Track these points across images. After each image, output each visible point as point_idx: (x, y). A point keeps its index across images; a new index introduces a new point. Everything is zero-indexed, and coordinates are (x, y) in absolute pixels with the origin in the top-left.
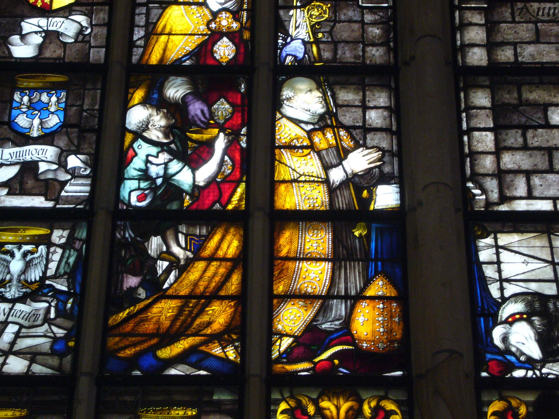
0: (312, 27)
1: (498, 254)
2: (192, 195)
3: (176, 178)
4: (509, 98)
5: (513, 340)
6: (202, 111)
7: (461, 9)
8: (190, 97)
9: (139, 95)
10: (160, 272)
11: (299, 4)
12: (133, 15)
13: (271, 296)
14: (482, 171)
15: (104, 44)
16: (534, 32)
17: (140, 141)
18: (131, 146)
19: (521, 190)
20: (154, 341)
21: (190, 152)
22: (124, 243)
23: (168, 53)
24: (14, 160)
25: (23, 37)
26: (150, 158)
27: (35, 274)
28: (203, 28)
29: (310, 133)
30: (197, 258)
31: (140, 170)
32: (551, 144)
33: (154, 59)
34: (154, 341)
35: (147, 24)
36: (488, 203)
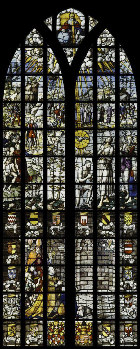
1: (79, 299)
4: (82, 270)
5: (80, 313)
8: (34, 271)
10: (32, 302)
14: (77, 285)
17: (27, 279)
18: (26, 280)
19: (83, 288)
20: (32, 314)
22: (27, 298)
24: (9, 283)
25: (8, 259)
27: (14, 303)
29: (52, 277)
30: (36, 300)
32: (88, 280)
34: (32, 314)
35: (27, 257)
36: (78, 291)
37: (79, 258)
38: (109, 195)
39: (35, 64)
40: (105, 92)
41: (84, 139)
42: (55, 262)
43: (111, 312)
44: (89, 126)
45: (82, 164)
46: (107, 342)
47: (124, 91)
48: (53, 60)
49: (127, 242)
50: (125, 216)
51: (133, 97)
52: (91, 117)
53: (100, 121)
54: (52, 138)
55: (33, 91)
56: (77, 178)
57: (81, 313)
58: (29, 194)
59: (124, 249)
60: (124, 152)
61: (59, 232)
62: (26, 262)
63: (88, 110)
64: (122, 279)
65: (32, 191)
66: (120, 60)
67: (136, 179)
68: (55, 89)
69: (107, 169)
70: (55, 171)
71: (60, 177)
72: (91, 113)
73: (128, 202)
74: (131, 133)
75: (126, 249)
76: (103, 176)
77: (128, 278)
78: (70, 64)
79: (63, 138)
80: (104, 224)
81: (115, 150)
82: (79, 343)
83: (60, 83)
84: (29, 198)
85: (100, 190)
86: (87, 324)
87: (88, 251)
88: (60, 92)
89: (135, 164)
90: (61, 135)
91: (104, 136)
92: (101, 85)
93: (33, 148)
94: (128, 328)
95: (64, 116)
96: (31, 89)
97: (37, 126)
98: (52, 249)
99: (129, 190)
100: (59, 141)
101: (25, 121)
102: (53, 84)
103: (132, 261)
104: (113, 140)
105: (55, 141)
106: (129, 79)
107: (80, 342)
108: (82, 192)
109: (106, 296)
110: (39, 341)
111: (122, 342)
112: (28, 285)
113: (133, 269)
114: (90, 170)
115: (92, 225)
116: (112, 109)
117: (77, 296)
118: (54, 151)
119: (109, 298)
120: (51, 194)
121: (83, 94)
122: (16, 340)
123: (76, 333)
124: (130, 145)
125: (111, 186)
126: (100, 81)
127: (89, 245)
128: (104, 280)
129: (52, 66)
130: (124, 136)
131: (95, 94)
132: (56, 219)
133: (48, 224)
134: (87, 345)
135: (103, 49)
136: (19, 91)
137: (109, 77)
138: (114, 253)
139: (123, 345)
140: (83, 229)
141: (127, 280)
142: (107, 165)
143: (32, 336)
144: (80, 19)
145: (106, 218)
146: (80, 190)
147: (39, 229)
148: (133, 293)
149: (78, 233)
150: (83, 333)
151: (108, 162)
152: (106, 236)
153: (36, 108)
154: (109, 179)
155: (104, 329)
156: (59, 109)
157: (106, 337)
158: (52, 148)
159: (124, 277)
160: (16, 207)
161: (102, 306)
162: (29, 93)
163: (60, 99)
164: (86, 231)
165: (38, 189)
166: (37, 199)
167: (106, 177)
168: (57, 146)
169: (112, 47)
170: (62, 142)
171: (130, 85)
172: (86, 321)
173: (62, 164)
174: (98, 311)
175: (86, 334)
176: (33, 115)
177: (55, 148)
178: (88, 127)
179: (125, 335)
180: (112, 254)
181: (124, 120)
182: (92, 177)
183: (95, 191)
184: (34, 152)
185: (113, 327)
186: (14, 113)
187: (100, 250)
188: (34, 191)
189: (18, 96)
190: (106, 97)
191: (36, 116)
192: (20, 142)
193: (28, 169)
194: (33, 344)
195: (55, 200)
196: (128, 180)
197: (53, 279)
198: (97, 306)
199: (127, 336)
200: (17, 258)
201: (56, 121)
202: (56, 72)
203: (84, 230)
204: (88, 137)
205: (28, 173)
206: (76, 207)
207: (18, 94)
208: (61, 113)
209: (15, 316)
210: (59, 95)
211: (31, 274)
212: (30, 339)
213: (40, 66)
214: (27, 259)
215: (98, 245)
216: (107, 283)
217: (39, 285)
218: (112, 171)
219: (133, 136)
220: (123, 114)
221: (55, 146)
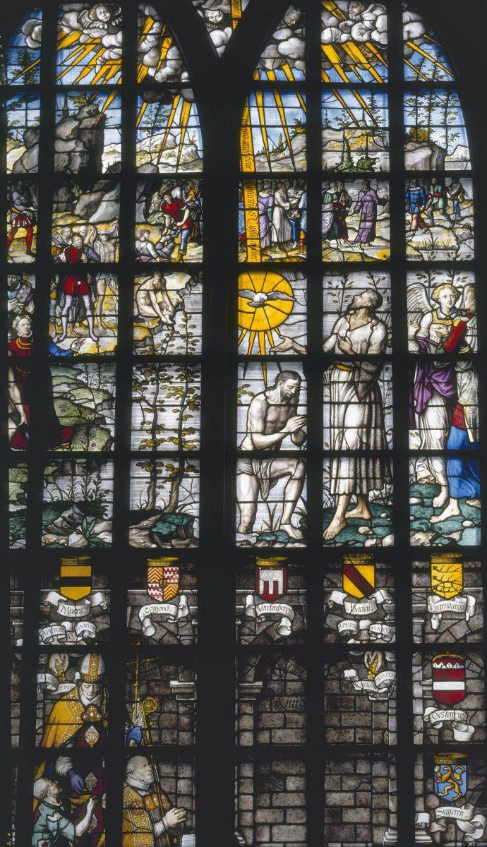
0: (146, 717)
2: (74, 843)
3: (64, 831)
4: (264, 770)
6: (79, 782)
7: (240, 702)
9: (42, 769)
11: (138, 700)
14: (244, 824)
15: (18, 732)
16: (283, 720)
21: (72, 812)
23: (57, 739)
26: (49, 817)
28: (78, 718)
31: (43, 826)
33: (49, 745)
37: (251, 722)
38: (371, 494)
39: (93, 54)
40: (351, 141)
41: (274, 300)
44: (289, 254)
45: (266, 385)
48: (157, 39)
49: (445, 661)
50: (435, 568)
51: (454, 157)
52: (300, 225)
53: (330, 235)
54: (152, 294)
55: (85, 139)
56: (247, 433)
58: (60, 490)
59: (432, 685)
60: (424, 342)
61: (172, 628)
63: (288, 201)
64: (425, 802)
65: (72, 480)
66: (405, 37)
67: (474, 437)
68: (165, 133)
70: (163, 410)
71: (180, 431)
72: (300, 211)
73: (442, 517)
74: (453, 277)
75: (440, 686)
76: (348, 424)
77: (453, 795)
78: (220, 50)
79: (192, 296)
80: (349, 595)
81: (393, 333)
83: (184, 113)
84: (60, 506)
85: (334, 476)
87: (286, 695)
89: (467, 386)
90: (188, 284)
91: (347, 286)
92: (337, 119)
93: (79, 330)
95: (198, 220)
96: (78, 134)
97: (95, 256)
98: (143, 688)
99: (446, 477)
100: (179, 307)
101: (50, 239)
102: (157, 115)
103: (466, 731)
104: (385, 302)
105: (164, 305)
106: (438, 100)
108: (265, 485)
112: (46, 826)
114: (296, 405)
115: (301, 601)
116: (377, 197)
118: (158, 339)
120: (145, 492)
121: (271, 150)
124: (448, 318)
125: (378, 464)
126: (331, 105)
127: (291, 673)
128: (352, 803)
129: (154, 58)
130: (425, 287)
131: (315, 148)
132: (164, 578)
133: (131, 597)
136: (33, 138)
138: (393, 704)
140: (269, 616)
141: (444, 802)
142: (360, 386)
145: (360, 574)
146: (256, 476)
147: (92, 616)
149: (247, 631)
151: (364, 376)
152: (356, 637)
153: (93, 197)
154: (368, 437)
158: (150, 330)
159: (433, 793)
163: (186, 164)
164: (280, 621)
165: (96, 473)
166: (91, 508)
167: (358, 428)
168: (170, 322)
170: (188, 307)
171: (445, 120)
173: (191, 385)
176: (81, 218)
177: (165, 327)
178: (288, 257)
180: (383, 708)
181: (425, 233)
182: (305, 429)
183: (313, 481)
184: (81, 343)
186: (12, 212)
187: (337, 691)
188: (79, 479)
189: (27, 154)
190: (356, 158)
191: (92, 220)
192: (31, 309)
193: (58, 406)
195: (160, 512)
196: (445, 440)
201: (168, 237)
202: (169, 77)
203: (274, 619)
204: (288, 290)
205: (56, 418)
206: (240, 537)
207: (29, 148)
208: (187, 213)
210: (180, 151)
213: (111, 59)
214: (44, 727)
215: (326, 674)
216: (364, 815)
218: (383, 409)
219: (461, 287)
220: (420, 213)
221: (161, 323)
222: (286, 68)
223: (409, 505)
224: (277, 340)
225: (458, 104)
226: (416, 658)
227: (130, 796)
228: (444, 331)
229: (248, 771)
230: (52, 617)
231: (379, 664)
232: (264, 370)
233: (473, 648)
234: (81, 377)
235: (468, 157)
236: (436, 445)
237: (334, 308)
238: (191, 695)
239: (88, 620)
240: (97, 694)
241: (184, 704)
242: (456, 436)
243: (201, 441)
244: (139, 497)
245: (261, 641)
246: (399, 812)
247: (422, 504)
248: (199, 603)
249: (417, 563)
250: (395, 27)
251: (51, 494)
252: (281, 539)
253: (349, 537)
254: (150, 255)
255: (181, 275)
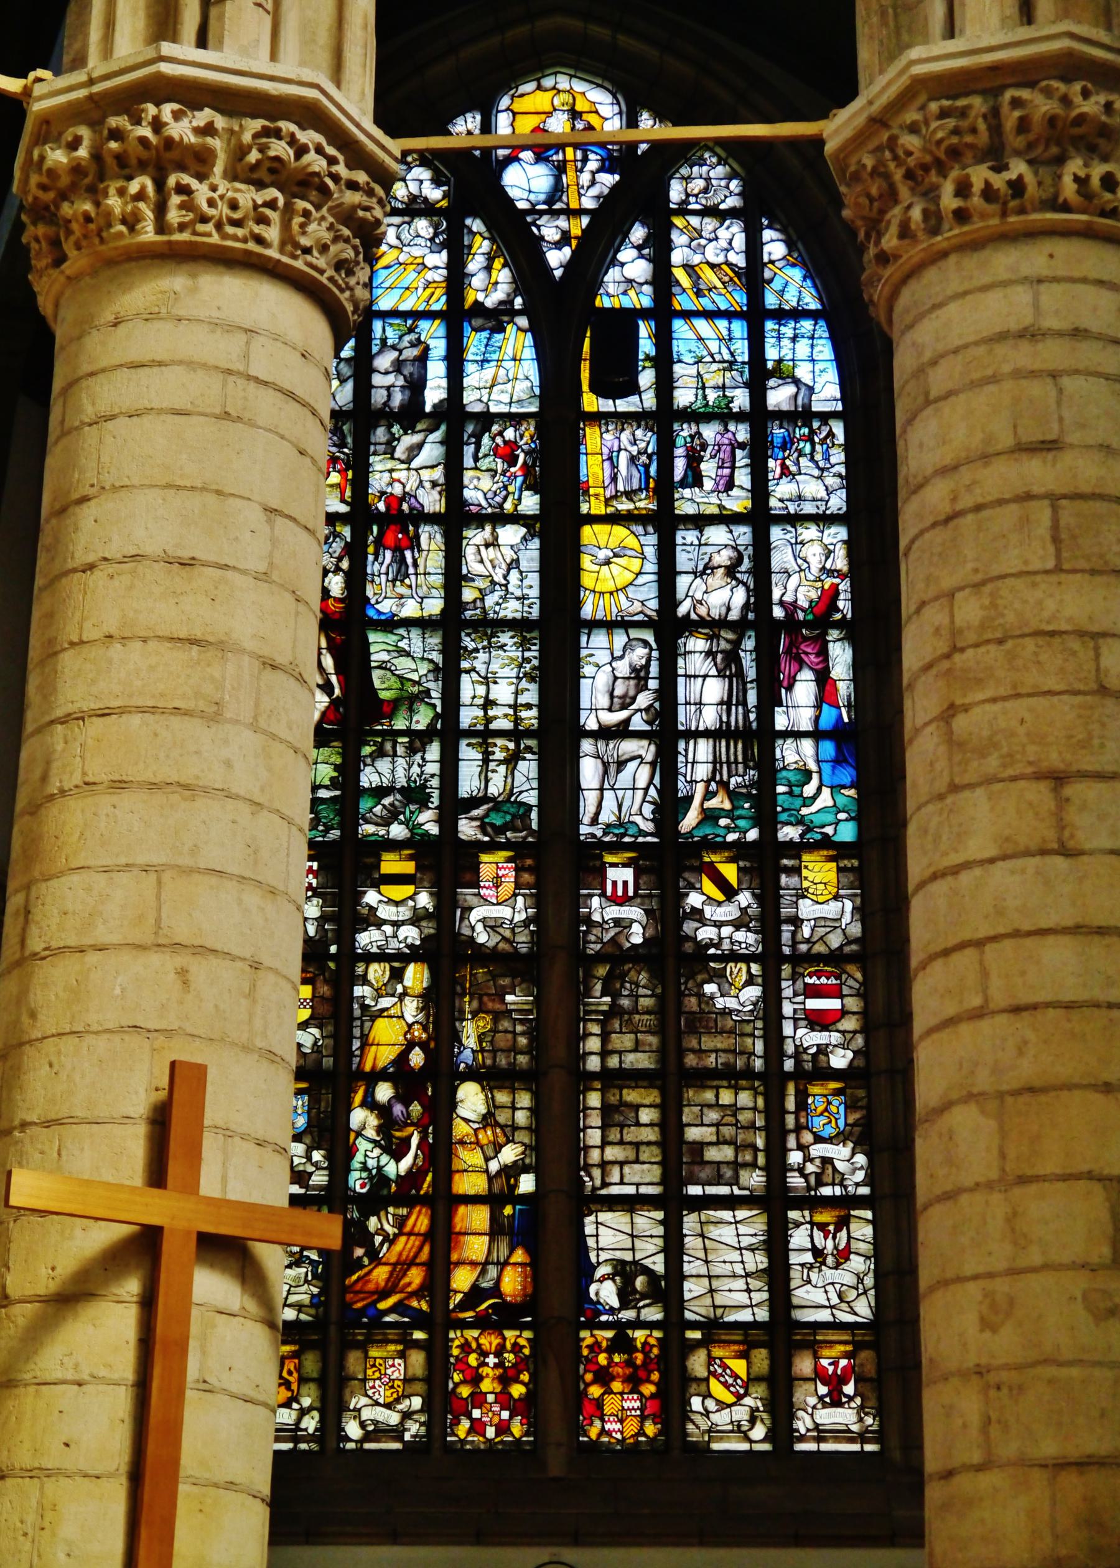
2: (396, 1182)
4: (613, 1099)
5: (602, 1294)
7: (586, 1021)
9: (358, 1098)
12: (351, 1027)
13: (449, 1263)
14: (591, 1162)
28: (401, 1038)
29: (476, 1130)
30: (401, 1234)
33: (368, 1067)
36: (594, 1189)
38: (733, 781)
40: (706, 376)
42: (489, 1062)
43: (748, 1291)
46: (732, 1431)
47: (783, 373)
51: (822, 396)
53: (683, 484)
54: (482, 549)
55: (406, 372)
57: (607, 1293)
60: (791, 608)
61: (508, 934)
62: (356, 1060)
64: (798, 1139)
65: (393, 762)
66: (766, 259)
67: (849, 717)
69: (721, 674)
70: (495, 683)
71: (515, 706)
72: (650, 457)
75: (813, 1004)
77: (829, 1131)
78: (558, 273)
80: (709, 898)
82: (599, 1435)
84: (380, 792)
85: (690, 759)
86: (639, 1345)
87: (638, 1013)
88: (520, 376)
89: (841, 656)
90: (524, 539)
93: (400, 589)
94: (835, 1364)
96: (398, 366)
98: (475, 1004)
99: (818, 762)
100: (514, 564)
101: (367, 485)
102: (487, 345)
104: (746, 561)
106: (803, 330)
107: (603, 1432)
108: (612, 769)
109: (726, 1215)
110: (409, 1424)
111: (803, 1431)
112: (365, 1163)
113: (848, 1091)
114: (647, 678)
117: (589, 1215)
118: (490, 601)
119: (736, 1222)
122: (299, 1420)
123: (582, 1386)
124: (818, 579)
125: (740, 746)
128: (714, 1139)
132: (498, 876)
133: (460, 897)
134: (637, 1443)
135: (695, 221)
137: (722, 324)
138: (759, 1024)
139: (811, 1446)
140: (617, 922)
141: (819, 1139)
142: (719, 657)
143: (377, 1404)
144: (596, 112)
147: (416, 919)
148: (846, 1203)
149: (592, 938)
150: (617, 1386)
151: (724, 645)
152: (717, 946)
153: (416, 438)
155: (720, 1371)
156: (516, 442)
157: (729, 1406)
158: (480, 590)
159: (807, 1128)
160: (321, 828)
161: (707, 1262)
162: (390, 379)
164: (630, 927)
165: (419, 754)
166: (415, 795)
169: (732, 213)
170: (524, 565)
172: (630, 1332)
173: (527, 654)
174: (687, 1285)
175: (630, 1393)
176: (402, 462)
179: (821, 1398)
180: (748, 1029)
182: (657, 705)
184: (402, 605)
185: (761, 1358)
187: (695, 1008)
190: (712, 396)
191: (414, 465)
192: (345, 565)
193: (376, 675)
194: (378, 1441)
195: (493, 799)
197: (476, 1136)
198: (682, 1261)
199: (827, 1400)
200: (316, 1040)
202: (501, 303)
205: (375, 691)
206: (584, 830)
209: (299, 1307)
211: (379, 1117)
212: (364, 1418)
214: (362, 1048)
216: (727, 1153)
217: (414, 1164)
218: (745, 683)
220: (784, 459)
221: (493, 583)
222: (632, 293)
223: (775, 795)
224: (625, 604)
225: (826, 335)
226: (786, 969)
227: (461, 1129)
228: (814, 595)
229: (594, 1099)
230: (373, 920)
231: (744, 978)
232: (610, 634)
233: (852, 958)
234: (403, 644)
235: (838, 396)
236: (806, 725)
237: (689, 567)
238: (529, 1012)
239: (413, 924)
240: (422, 1009)
241: (522, 1022)
242: (828, 716)
243: (540, 718)
244: (468, 783)
245: (609, 949)
246: (767, 1150)
247: (790, 793)
248: (538, 905)
249: (785, 862)
250: (754, 248)
251: (369, 778)
252: (630, 832)
253: (708, 830)
254: (480, 505)
255: (515, 527)
